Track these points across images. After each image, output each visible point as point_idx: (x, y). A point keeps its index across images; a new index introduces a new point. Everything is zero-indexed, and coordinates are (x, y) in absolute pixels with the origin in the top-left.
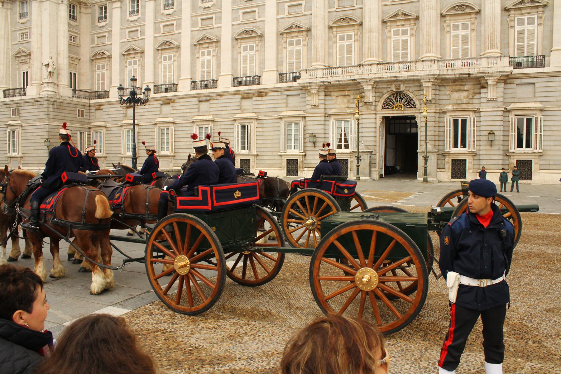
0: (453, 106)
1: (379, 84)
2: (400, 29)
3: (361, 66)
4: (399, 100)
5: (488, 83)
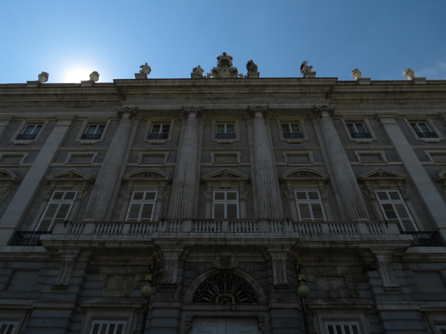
1: (194, 254)
2: (226, 192)
3: (165, 222)
4: (225, 286)
5: (379, 260)
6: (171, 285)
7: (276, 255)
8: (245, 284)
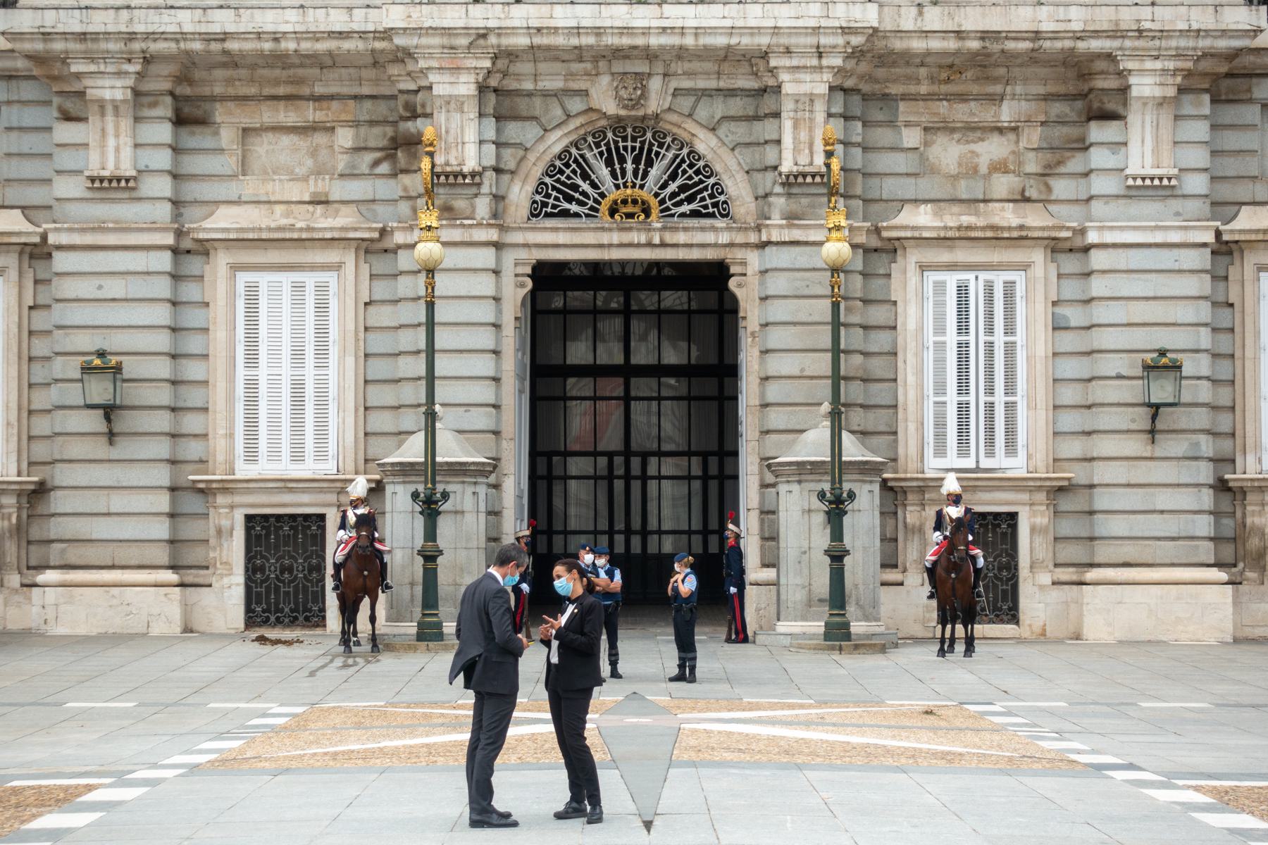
0: (935, 214)
1: (525, 67)
4: (629, 167)
5: (1135, 92)
6: (464, 177)
7: (797, 76)
8: (694, 157)
